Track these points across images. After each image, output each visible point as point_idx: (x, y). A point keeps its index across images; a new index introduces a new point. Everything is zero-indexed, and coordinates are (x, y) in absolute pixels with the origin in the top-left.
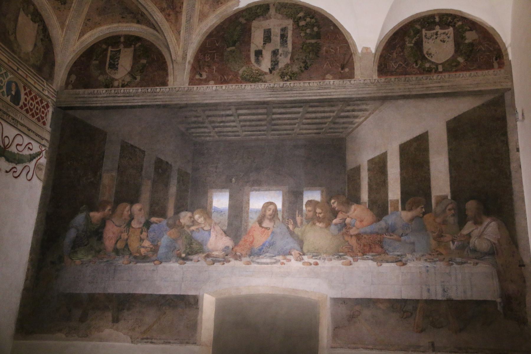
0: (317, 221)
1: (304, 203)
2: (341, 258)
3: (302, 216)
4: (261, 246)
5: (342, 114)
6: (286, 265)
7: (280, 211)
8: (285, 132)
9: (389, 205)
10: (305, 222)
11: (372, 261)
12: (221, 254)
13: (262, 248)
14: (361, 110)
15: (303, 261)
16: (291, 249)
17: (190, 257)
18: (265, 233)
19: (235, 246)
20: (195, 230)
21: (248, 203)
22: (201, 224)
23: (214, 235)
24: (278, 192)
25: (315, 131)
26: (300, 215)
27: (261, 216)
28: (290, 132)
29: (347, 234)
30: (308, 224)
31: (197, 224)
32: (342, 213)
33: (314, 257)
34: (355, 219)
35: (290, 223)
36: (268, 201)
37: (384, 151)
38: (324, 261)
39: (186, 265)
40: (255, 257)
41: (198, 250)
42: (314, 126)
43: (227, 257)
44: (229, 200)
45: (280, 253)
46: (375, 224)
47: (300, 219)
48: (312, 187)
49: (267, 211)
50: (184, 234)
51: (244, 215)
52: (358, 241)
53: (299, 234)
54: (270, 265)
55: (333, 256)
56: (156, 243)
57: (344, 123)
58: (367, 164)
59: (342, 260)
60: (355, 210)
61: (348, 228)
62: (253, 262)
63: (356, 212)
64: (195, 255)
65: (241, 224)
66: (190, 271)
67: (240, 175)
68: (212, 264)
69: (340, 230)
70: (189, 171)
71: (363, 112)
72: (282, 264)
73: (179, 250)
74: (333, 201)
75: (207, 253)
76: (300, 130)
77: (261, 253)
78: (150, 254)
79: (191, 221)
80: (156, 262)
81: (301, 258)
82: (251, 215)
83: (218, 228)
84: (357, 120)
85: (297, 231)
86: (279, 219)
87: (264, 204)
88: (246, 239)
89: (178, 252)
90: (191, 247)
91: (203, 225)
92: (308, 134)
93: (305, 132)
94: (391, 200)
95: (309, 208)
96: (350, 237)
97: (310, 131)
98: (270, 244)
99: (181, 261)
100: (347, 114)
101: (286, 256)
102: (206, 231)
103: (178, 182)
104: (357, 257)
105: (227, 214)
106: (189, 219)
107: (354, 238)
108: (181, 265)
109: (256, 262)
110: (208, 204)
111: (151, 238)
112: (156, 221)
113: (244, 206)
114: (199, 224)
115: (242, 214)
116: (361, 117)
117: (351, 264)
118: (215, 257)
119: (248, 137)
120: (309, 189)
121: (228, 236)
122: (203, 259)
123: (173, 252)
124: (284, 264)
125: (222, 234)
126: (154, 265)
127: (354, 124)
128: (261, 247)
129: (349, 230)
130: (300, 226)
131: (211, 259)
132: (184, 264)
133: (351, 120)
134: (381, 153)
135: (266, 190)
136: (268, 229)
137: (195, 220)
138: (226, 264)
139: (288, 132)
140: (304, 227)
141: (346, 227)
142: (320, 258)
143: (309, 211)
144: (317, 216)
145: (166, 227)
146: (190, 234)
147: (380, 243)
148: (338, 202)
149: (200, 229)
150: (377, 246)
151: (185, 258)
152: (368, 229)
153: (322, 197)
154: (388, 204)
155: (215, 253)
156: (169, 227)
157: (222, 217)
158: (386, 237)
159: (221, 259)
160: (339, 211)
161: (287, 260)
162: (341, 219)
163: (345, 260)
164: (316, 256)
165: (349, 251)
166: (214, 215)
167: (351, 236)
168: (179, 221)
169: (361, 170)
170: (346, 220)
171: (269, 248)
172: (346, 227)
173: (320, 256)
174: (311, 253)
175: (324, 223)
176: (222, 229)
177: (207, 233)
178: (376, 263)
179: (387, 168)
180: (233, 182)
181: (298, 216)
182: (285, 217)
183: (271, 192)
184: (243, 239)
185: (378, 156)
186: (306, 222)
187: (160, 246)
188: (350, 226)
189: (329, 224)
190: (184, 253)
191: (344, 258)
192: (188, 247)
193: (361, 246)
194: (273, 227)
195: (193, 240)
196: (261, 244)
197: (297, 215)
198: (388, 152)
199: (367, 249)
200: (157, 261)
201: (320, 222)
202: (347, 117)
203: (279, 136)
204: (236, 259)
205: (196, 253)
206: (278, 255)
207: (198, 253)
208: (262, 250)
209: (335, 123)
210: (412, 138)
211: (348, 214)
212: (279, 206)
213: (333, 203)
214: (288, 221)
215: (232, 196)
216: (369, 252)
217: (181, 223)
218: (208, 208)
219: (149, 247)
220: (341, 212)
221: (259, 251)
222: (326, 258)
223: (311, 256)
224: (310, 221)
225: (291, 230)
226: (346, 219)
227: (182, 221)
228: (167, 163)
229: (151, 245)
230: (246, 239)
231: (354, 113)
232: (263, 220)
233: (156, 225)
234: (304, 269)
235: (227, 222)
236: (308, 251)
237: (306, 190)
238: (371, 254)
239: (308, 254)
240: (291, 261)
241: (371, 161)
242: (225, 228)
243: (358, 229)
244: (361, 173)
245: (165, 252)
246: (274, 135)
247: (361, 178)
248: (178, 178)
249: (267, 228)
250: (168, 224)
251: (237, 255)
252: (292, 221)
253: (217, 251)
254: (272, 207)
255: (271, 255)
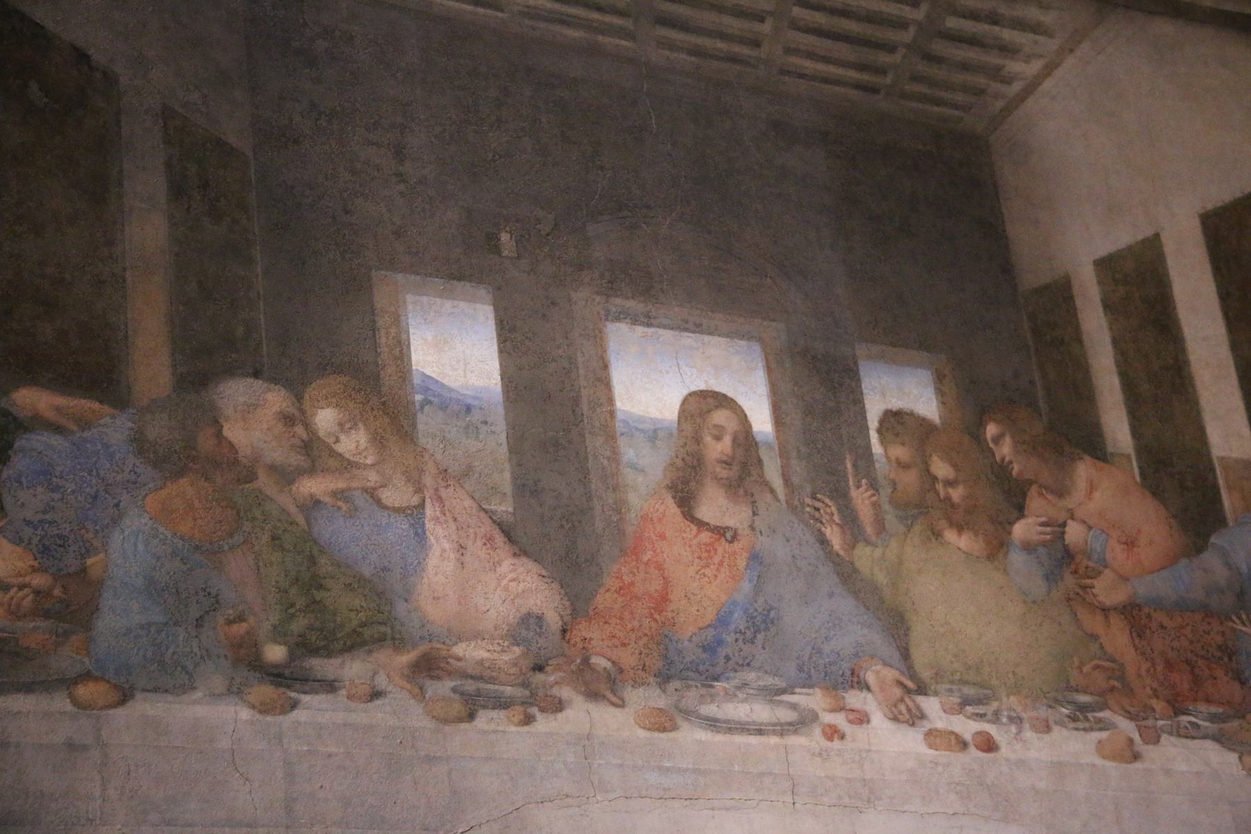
0: (943, 523)
1: (873, 422)
2: (1087, 719)
3: (874, 486)
4: (709, 626)
5: (952, 23)
6: (848, 744)
7: (769, 446)
8: (721, 45)
9: (1221, 482)
10: (891, 519)
11: (1217, 746)
12: (506, 657)
13: (720, 642)
14: (1021, 25)
15: (927, 726)
16: (856, 655)
17: (323, 667)
18: (717, 560)
19: (575, 613)
20: (327, 499)
21: (603, 381)
22: (357, 466)
23: (447, 546)
24: (743, 343)
25: (853, 74)
26: (864, 481)
27: (679, 463)
28: (745, 51)
29: (1084, 599)
30: (909, 528)
31: (332, 463)
32: (1041, 494)
33: (969, 709)
34: (1103, 531)
35: (825, 518)
36: (702, 387)
37: (1149, 232)
38: (1017, 734)
39: (299, 715)
40: (688, 687)
41: (363, 625)
42: (844, 51)
43: (539, 677)
44: (501, 351)
45: (810, 676)
46: (1184, 561)
47: (867, 502)
48: (893, 345)
49: (708, 439)
50: (257, 513)
51: (595, 443)
52: (1137, 641)
53: (881, 578)
54: (774, 740)
55: (1050, 707)
56: (72, 564)
57: (965, 67)
58: (1095, 281)
59: (1092, 729)
60: (1092, 488)
61: (1082, 570)
62: (688, 714)
63: (1097, 495)
64: (347, 656)
65: (589, 499)
66: (330, 756)
67: (538, 221)
68: (460, 720)
69: (1051, 578)
70: (235, 131)
71: (1031, 36)
72: (830, 739)
73: (241, 619)
74: (991, 430)
75: (423, 648)
76: (788, 51)
77: (718, 669)
78: (35, 633)
79: (296, 441)
80: (82, 691)
81: (914, 711)
82: (629, 453)
83: (461, 502)
84: (1014, 66)
85: (864, 557)
86: (772, 491)
87: (685, 401)
88: (627, 579)
89: (239, 629)
90: (315, 606)
91: (373, 477)
92: (826, 80)
93: (810, 66)
94: (1222, 459)
95: (899, 452)
96: (1099, 617)
97: (832, 70)
98: (752, 618)
99: (266, 691)
100: (968, 26)
101: (841, 693)
102: (398, 510)
103: (178, 191)
104: (1150, 722)
105: (501, 427)
106: (280, 427)
107: (1116, 621)
108: (269, 718)
109: (699, 717)
110: (384, 349)
111: (28, 523)
112: (50, 415)
113: (584, 392)
114: (347, 466)
115: (582, 435)
116: (1028, 59)
117: (1136, 757)
118: (472, 677)
119: (542, 25)
120: (881, 357)
121: (525, 553)
122: (408, 686)
123: (199, 623)
124: (842, 737)
125: (490, 539)
126: (69, 707)
127: (1008, 81)
128: (711, 632)
129: (1088, 582)
130: (874, 538)
131: (447, 685)
132: (284, 712)
133: (993, 59)
134: (1140, 237)
135: (683, 326)
136: (729, 535)
137: (319, 438)
138: (544, 724)
139: (737, 49)
140: (894, 544)
141: (1073, 567)
142: (997, 714)
143: (901, 465)
144: (942, 496)
145: (131, 460)
146: (300, 519)
147: (1230, 660)
148: (1013, 437)
149: (360, 500)
150: (1220, 673)
151: (287, 672)
152: (1162, 585)
153: (943, 403)
154: (1215, 478)
155: (472, 652)
156: (156, 464)
157: (477, 438)
158: (1244, 629)
159: (508, 690)
160: (1030, 483)
161: (851, 717)
162: (1042, 524)
163: (1104, 735)
164: (980, 701)
165: (1112, 689)
166: (428, 423)
167: (1105, 611)
168: (219, 434)
169: (1079, 302)
170: (1067, 529)
171: (752, 642)
172: (1073, 567)
173: (995, 705)
174: (955, 687)
175: (976, 534)
176: (486, 511)
177: (402, 525)
178: (1233, 757)
179: (1175, 308)
180: (505, 253)
181: (858, 487)
182: (795, 480)
183: (707, 338)
184: (610, 582)
185: (1130, 248)
186: (901, 519)
187: (101, 582)
188: (1091, 564)
189: (1002, 544)
190: (275, 642)
191: (1100, 720)
192: (301, 602)
193: (1154, 665)
194: (752, 528)
195: (323, 561)
196: (710, 615)
197: (851, 483)
198: (1163, 240)
199: (1182, 681)
200: (96, 679)
201: (960, 529)
202: (973, 41)
203: (693, 59)
204: (593, 695)
205: (356, 643)
206: (804, 687)
207: (363, 643)
208: (722, 652)
209: (931, 58)
210: (1238, 194)
211: (1069, 503)
212: (762, 422)
213: (997, 439)
214: (818, 504)
215: (513, 329)
216: (1195, 700)
217: (232, 445)
218: (389, 376)
219: (21, 587)
220: (1034, 489)
221: (704, 656)
222: (1024, 715)
223: (956, 700)
224: (915, 518)
225: (838, 555)
226: (1064, 525)
227: (233, 432)
228: (81, 56)
229: (34, 570)
230: (627, 579)
231: (997, 28)
232: (693, 484)
233: (55, 440)
234: (940, 769)
235: (507, 475)
236: (938, 676)
237: (869, 357)
238: (1203, 708)
239: (939, 687)
240: (868, 721)
241: (1105, 265)
242: (505, 508)
243: (1124, 579)
244: (1080, 316)
245: (142, 627)
246: (672, 46)
247: (1085, 337)
248: (168, 165)
249: (728, 528)
250: (139, 443)
251: (593, 670)
252: (834, 509)
253: (477, 636)
254: (721, 417)
255: (769, 681)
